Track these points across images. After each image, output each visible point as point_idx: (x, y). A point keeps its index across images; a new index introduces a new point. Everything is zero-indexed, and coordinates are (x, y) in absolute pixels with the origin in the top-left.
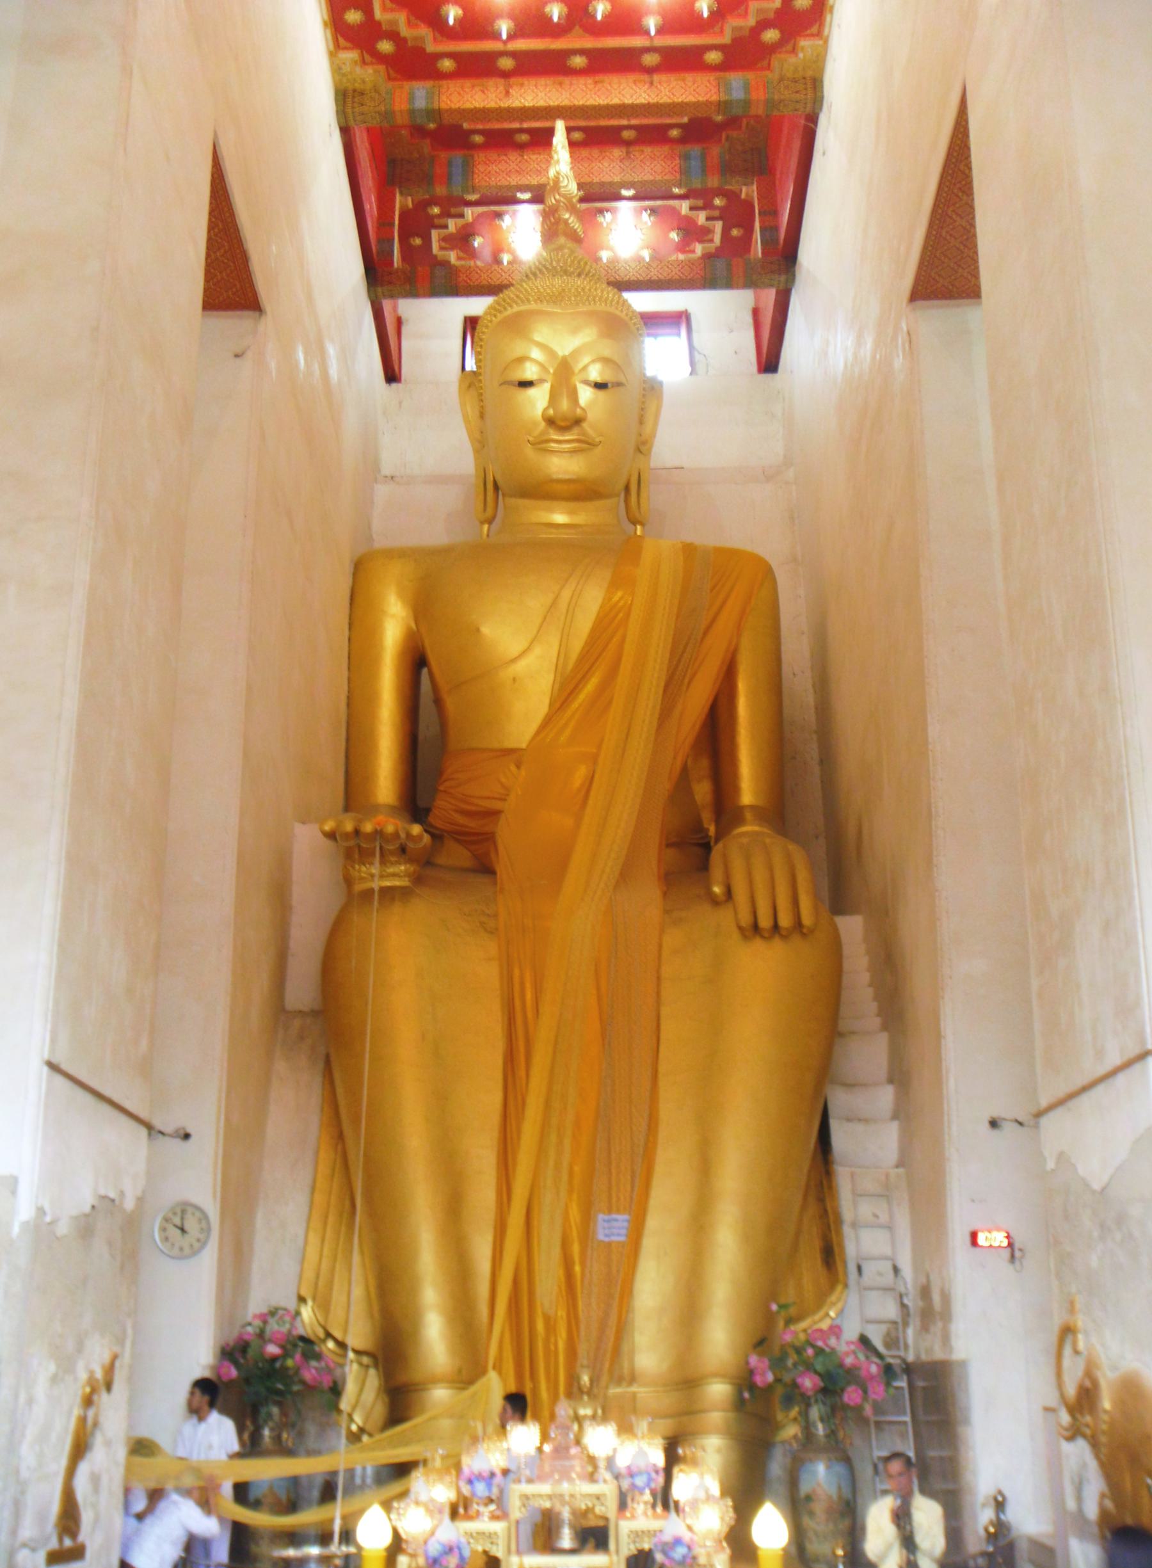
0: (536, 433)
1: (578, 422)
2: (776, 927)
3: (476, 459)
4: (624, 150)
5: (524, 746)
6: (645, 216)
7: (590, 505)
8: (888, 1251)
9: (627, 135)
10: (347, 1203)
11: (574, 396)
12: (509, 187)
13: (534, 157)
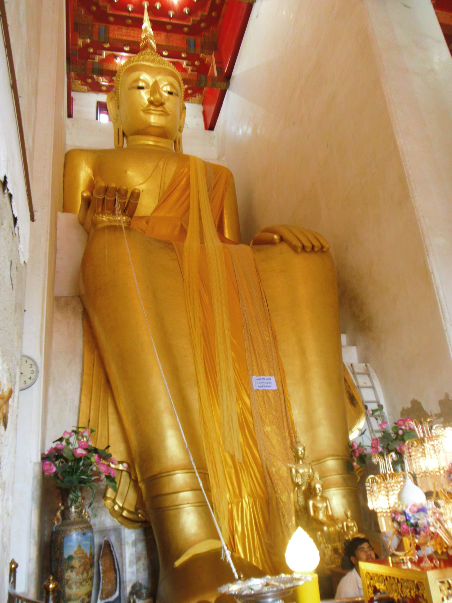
0: (145, 107)
1: (162, 104)
2: (313, 247)
3: (114, 126)
4: (166, 34)
5: (149, 215)
8: (374, 399)
9: (169, 27)
10: (103, 381)
11: (161, 95)
12: (122, 41)
13: (132, 31)
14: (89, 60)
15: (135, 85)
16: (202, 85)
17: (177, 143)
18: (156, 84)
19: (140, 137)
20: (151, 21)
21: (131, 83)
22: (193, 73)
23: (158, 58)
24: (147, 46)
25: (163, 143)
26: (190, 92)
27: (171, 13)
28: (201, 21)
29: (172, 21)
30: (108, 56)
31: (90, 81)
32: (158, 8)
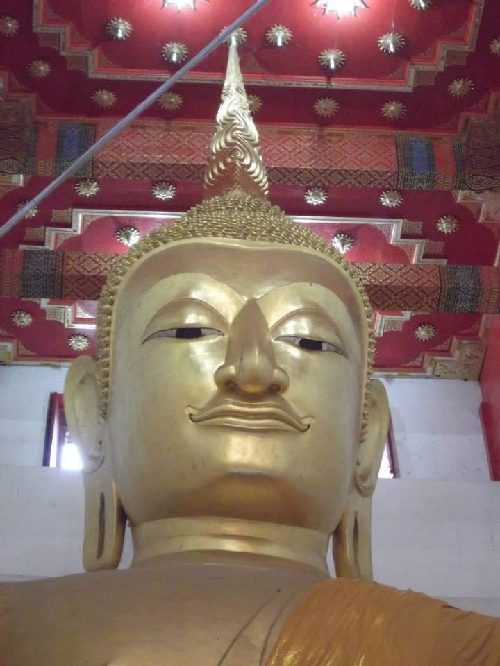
0: (201, 405)
1: (275, 390)
4: (314, 130)
6: (337, 243)
7: (286, 531)
9: (325, 107)
11: (270, 353)
14: (22, 247)
15: (171, 322)
16: (462, 306)
17: (347, 536)
18: (251, 313)
19: (181, 523)
20: (250, 90)
21: (153, 320)
22: (431, 261)
23: (276, 217)
24: (232, 177)
25: (279, 544)
26: (422, 333)
27: (332, 58)
28: (452, 73)
29: (337, 84)
30: (93, 228)
31: (25, 320)
32: (280, 43)
